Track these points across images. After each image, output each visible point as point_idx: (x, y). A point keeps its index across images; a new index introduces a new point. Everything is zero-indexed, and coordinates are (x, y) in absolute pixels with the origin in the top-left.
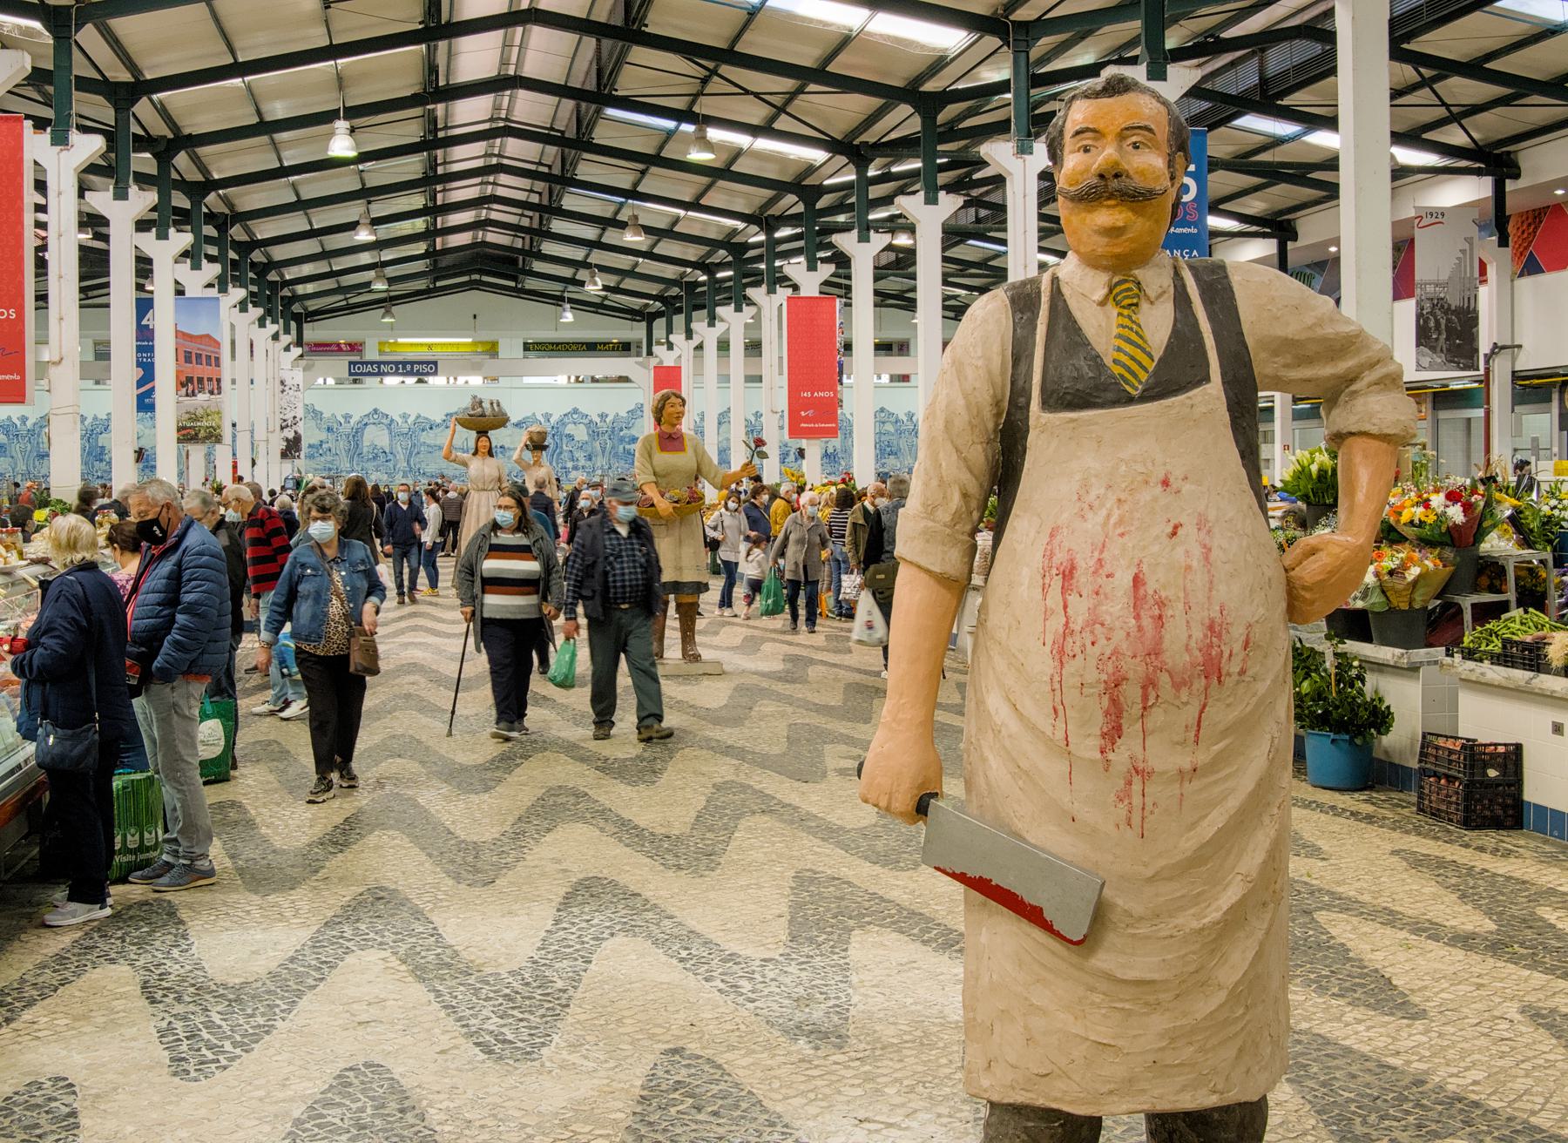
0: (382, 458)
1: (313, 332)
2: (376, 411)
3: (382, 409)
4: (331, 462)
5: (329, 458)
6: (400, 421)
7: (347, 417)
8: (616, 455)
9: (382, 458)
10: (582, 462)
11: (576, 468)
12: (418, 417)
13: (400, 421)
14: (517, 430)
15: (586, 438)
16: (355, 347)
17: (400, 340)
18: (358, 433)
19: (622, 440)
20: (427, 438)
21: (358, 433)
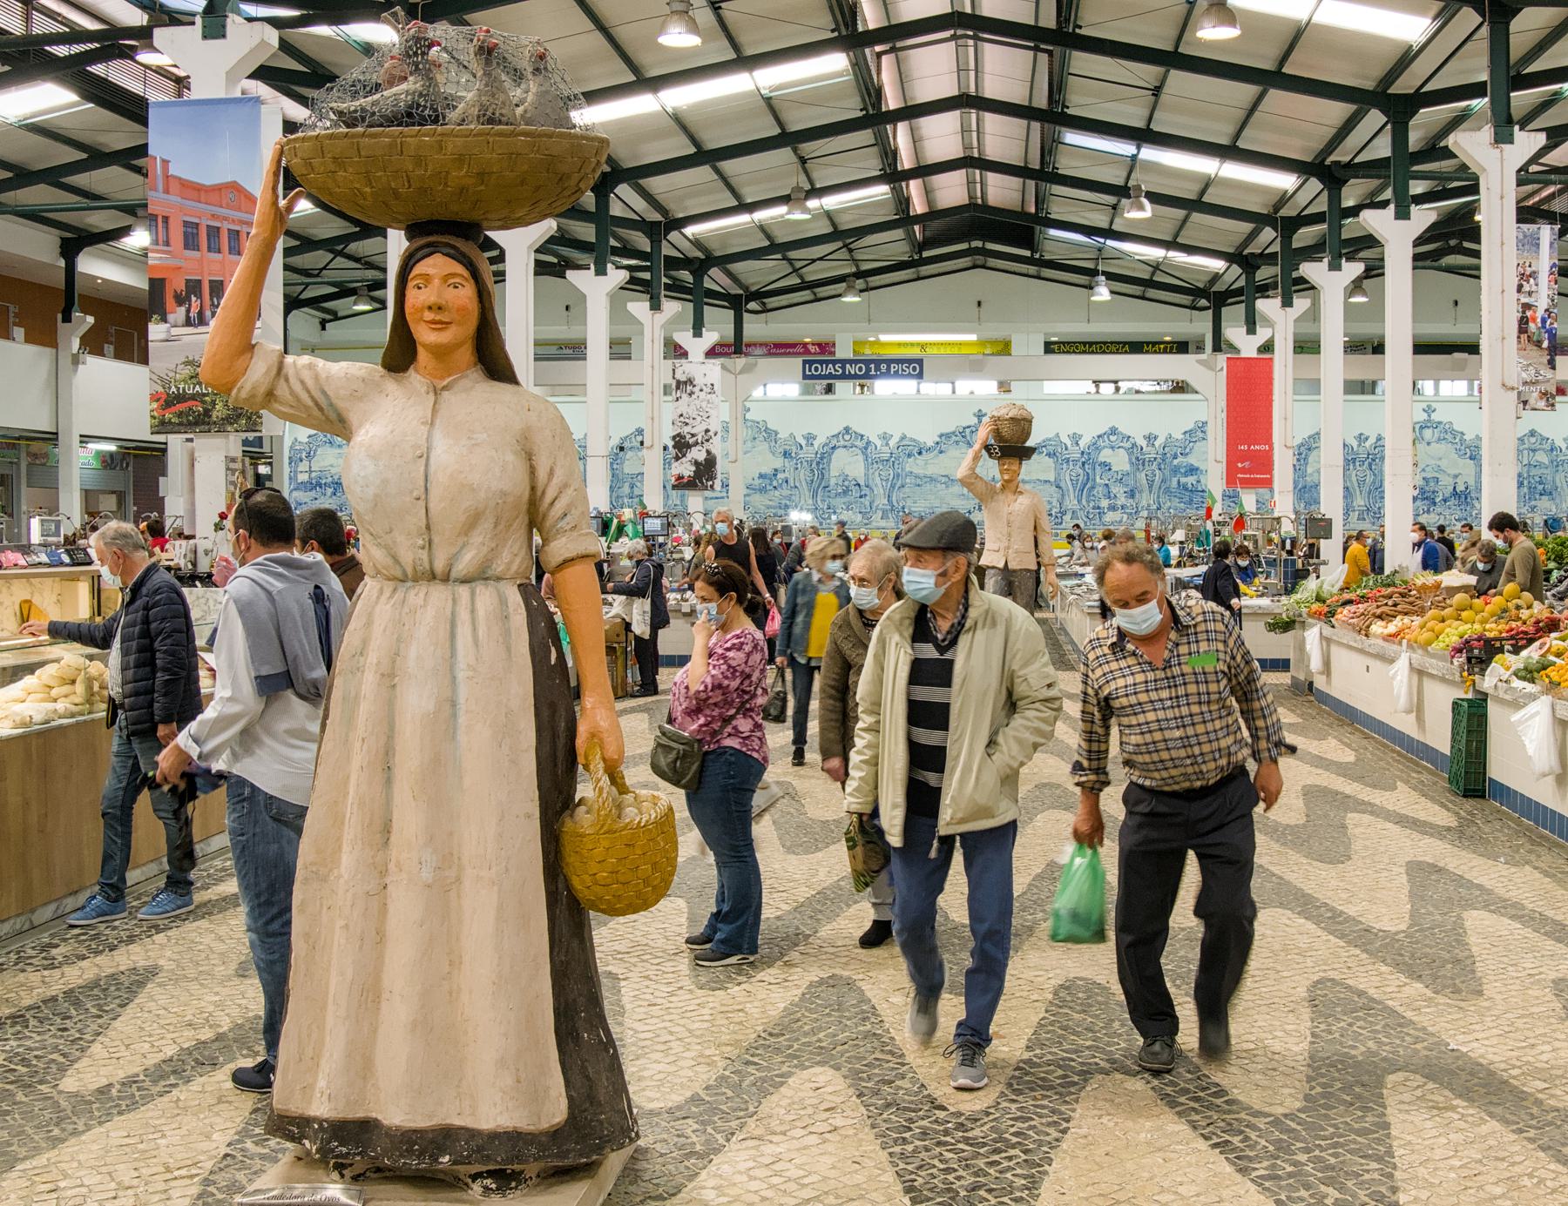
0: (855, 492)
1: (755, 328)
2: (847, 430)
5: (786, 492)
6: (879, 443)
7: (810, 438)
8: (1168, 491)
9: (855, 492)
10: (1122, 500)
11: (1113, 508)
12: (903, 438)
13: (879, 443)
15: (1127, 467)
16: (825, 347)
17: (884, 338)
18: (823, 458)
19: (1175, 470)
20: (915, 466)
21: (823, 458)
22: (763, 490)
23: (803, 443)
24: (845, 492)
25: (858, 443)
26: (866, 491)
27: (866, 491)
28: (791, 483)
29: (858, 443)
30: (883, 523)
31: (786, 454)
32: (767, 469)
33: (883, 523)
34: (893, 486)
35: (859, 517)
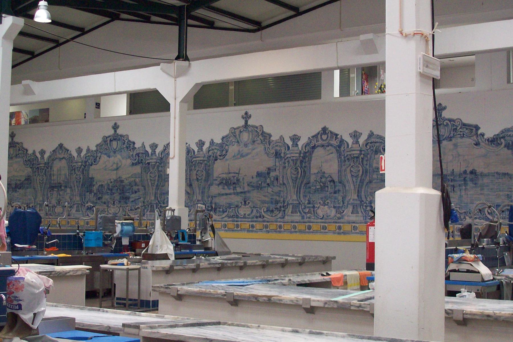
2: (324, 130)
3: (333, 128)
4: (278, 194)
5: (276, 189)
6: (350, 141)
7: (295, 139)
13: (350, 141)
14: (492, 148)
18: (306, 156)
21: (306, 156)
22: (259, 187)
23: (290, 143)
25: (334, 142)
26: (339, 187)
29: (334, 142)
30: (353, 218)
31: (277, 155)
32: (262, 169)
33: (353, 218)
34: (362, 181)
35: (334, 211)
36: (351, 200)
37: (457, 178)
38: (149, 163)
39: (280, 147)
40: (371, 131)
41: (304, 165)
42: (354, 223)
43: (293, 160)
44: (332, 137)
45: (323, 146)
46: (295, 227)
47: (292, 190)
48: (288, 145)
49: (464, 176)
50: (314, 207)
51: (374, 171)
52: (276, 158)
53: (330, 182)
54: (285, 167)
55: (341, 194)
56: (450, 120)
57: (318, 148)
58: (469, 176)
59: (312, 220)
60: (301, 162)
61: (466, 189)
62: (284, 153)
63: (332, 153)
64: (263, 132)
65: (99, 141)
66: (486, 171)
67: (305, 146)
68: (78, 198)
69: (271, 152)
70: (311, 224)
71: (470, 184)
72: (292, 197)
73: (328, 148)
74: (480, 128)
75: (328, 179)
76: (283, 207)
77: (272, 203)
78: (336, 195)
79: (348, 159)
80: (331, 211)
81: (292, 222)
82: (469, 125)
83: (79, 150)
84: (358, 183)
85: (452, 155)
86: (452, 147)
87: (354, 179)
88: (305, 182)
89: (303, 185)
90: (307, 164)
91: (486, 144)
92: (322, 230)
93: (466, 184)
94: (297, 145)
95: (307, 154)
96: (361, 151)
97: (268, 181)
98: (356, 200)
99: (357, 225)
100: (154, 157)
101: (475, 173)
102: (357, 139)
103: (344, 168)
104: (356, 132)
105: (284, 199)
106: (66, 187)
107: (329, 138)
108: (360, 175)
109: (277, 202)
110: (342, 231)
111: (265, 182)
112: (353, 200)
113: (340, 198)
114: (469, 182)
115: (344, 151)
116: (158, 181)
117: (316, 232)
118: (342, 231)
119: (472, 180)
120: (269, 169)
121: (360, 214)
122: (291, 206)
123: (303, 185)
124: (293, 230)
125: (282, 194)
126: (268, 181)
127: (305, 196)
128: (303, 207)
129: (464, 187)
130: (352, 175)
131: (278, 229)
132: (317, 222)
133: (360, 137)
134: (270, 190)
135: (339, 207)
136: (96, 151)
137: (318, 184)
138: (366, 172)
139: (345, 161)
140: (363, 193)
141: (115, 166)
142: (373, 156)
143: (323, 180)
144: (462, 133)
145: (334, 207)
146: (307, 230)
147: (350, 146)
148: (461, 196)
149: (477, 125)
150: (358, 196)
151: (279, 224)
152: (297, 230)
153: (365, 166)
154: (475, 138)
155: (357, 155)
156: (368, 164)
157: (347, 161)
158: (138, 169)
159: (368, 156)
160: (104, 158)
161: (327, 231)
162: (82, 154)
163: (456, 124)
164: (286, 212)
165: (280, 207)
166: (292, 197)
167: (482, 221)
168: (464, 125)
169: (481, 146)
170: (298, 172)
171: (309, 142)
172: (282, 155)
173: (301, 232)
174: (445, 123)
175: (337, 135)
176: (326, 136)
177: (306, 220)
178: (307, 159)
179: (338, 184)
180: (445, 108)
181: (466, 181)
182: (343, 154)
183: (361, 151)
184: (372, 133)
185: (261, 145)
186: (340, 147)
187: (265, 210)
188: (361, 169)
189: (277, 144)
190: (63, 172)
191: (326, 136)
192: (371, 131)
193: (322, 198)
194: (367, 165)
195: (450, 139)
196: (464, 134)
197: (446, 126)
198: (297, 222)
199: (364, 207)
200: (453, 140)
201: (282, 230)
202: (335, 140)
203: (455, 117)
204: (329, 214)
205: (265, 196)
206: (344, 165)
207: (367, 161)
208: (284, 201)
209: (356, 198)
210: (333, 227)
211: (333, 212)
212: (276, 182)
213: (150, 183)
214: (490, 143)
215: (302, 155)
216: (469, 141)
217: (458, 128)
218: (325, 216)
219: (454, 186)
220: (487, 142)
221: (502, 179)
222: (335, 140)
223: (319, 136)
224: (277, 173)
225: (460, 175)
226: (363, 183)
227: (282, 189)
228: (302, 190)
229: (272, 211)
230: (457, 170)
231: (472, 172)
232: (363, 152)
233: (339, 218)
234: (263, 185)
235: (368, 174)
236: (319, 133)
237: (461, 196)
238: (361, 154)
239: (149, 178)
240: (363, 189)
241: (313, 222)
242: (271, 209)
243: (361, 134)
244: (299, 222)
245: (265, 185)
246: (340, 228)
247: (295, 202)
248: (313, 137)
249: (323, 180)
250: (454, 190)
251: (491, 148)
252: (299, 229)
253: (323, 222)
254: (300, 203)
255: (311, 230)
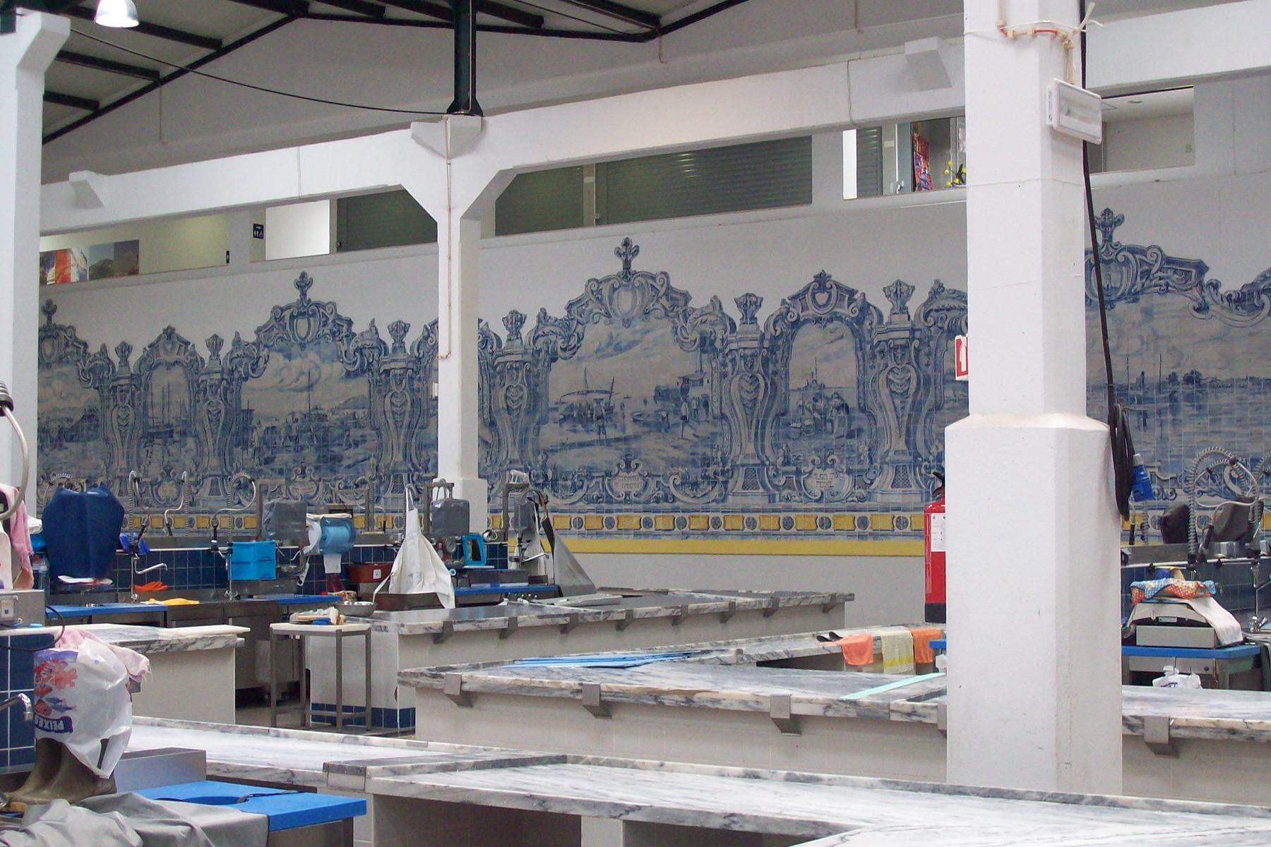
2: (822, 281)
3: (841, 275)
4: (710, 440)
5: (705, 429)
6: (885, 306)
7: (749, 304)
13: (885, 306)
14: (1241, 317)
22: (661, 426)
23: (736, 315)
24: (820, 426)
26: (860, 421)
27: (860, 421)
28: (715, 407)
30: (896, 497)
31: (705, 344)
32: (669, 380)
33: (896, 497)
34: (916, 407)
35: (848, 481)
36: (891, 454)
37: (1154, 394)
38: (387, 372)
39: (713, 324)
40: (936, 281)
41: (771, 368)
42: (898, 509)
43: (744, 357)
44: (840, 299)
45: (818, 320)
46: (752, 523)
47: (744, 431)
48: (730, 319)
49: (1170, 387)
50: (798, 473)
51: (945, 382)
52: (703, 351)
53: (838, 408)
54: (725, 375)
55: (865, 437)
56: (1133, 250)
57: (808, 325)
58: (1181, 389)
59: (794, 505)
60: (766, 362)
61: (1174, 422)
62: (723, 340)
63: (841, 338)
64: (669, 287)
65: (264, 318)
66: (1224, 376)
67: (775, 322)
68: (214, 462)
69: (692, 338)
70: (793, 515)
71: (1186, 408)
72: (744, 449)
73: (830, 326)
74: (1208, 268)
75: (832, 403)
76: (723, 473)
77: (694, 462)
78: (854, 442)
79: (882, 352)
80: (842, 481)
81: (743, 511)
82: (1182, 263)
83: (215, 343)
84: (907, 412)
85: (1141, 337)
86: (1138, 317)
87: (897, 402)
88: (772, 414)
89: (770, 419)
90: (779, 365)
91: (1222, 307)
92: (819, 529)
93: (1174, 409)
94: (754, 319)
95: (780, 342)
96: (913, 330)
97: (684, 410)
98: (903, 452)
99: (907, 515)
100: (401, 356)
101: (1198, 381)
102: (904, 303)
103: (871, 374)
104: (899, 283)
105: (723, 453)
106: (184, 434)
107: (833, 301)
108: (912, 391)
109: (707, 461)
110: (869, 530)
111: (676, 413)
112: (896, 452)
113: (864, 449)
114: (1183, 404)
115: (870, 332)
116: (411, 415)
117: (805, 534)
118: (869, 530)
119: (1189, 398)
120: (686, 380)
121: (914, 488)
122: (742, 471)
123: (770, 419)
124: (746, 530)
125: (719, 441)
126: (684, 410)
127: (776, 446)
128: (771, 473)
129: (1170, 417)
130: (892, 392)
131: (711, 529)
132: (806, 510)
133: (909, 296)
134: (688, 432)
135: (861, 471)
136: (257, 344)
137: (807, 412)
138: (927, 381)
139: (874, 356)
140: (919, 438)
141: (304, 381)
142: (943, 341)
143: (821, 404)
144: (1162, 282)
145: (849, 472)
146: (783, 530)
147: (886, 320)
148: (1162, 439)
149: (1201, 262)
150: (907, 442)
151: (711, 515)
152: (757, 530)
153: (923, 367)
154: (1195, 293)
155: (903, 342)
156: (932, 362)
157: (878, 357)
158: (360, 387)
159: (932, 343)
160: (277, 360)
161: (831, 530)
162: (223, 353)
163: (1149, 259)
164: (730, 486)
165: (715, 473)
166: (744, 449)
167: (1217, 498)
168: (1169, 261)
169: (1210, 313)
170: (758, 387)
171: (784, 310)
172: (718, 344)
173: (767, 534)
174: (1121, 258)
175: (852, 293)
176: (826, 295)
177: (780, 505)
178: (779, 353)
179: (857, 414)
180: (1120, 221)
181: (1176, 400)
182: (868, 339)
183: (913, 330)
184: (941, 286)
185: (665, 321)
186: (860, 321)
187: (678, 482)
188: (913, 374)
189: (704, 318)
190: (175, 397)
191: (826, 295)
192: (936, 281)
193: (817, 450)
194: (927, 365)
195: (1134, 297)
196: (1167, 285)
197: (1123, 264)
198: (757, 511)
199: (923, 471)
200: (1143, 299)
201: (721, 529)
202: (849, 305)
203: (1144, 243)
204: (835, 489)
205: (675, 447)
206: (872, 367)
207: (928, 355)
208: (724, 461)
209: (901, 445)
210: (846, 521)
211: (845, 485)
212: (702, 411)
213: (391, 422)
214: (1233, 305)
215: (766, 344)
216: (1180, 302)
217: (1154, 270)
218: (826, 496)
219: (1145, 415)
220: (1226, 303)
221: (1265, 393)
222: (849, 305)
223: (808, 296)
224: (706, 389)
225: (1160, 387)
226: (919, 411)
227: (717, 430)
228: (768, 430)
229: (695, 485)
230: (1152, 375)
231: (1189, 380)
232: (918, 334)
233: (862, 499)
234: (673, 419)
235: (932, 387)
236: (806, 290)
237: (1162, 439)
238: (914, 339)
239: (388, 407)
240: (920, 426)
241: (795, 511)
242: (692, 479)
243: (913, 288)
244: (764, 511)
245: (678, 420)
246: (863, 523)
247: (751, 461)
248: (794, 298)
249: (821, 404)
250: (1145, 424)
251: (1238, 318)
252: (763, 526)
253: (821, 510)
254: (763, 464)
255: (793, 530)
